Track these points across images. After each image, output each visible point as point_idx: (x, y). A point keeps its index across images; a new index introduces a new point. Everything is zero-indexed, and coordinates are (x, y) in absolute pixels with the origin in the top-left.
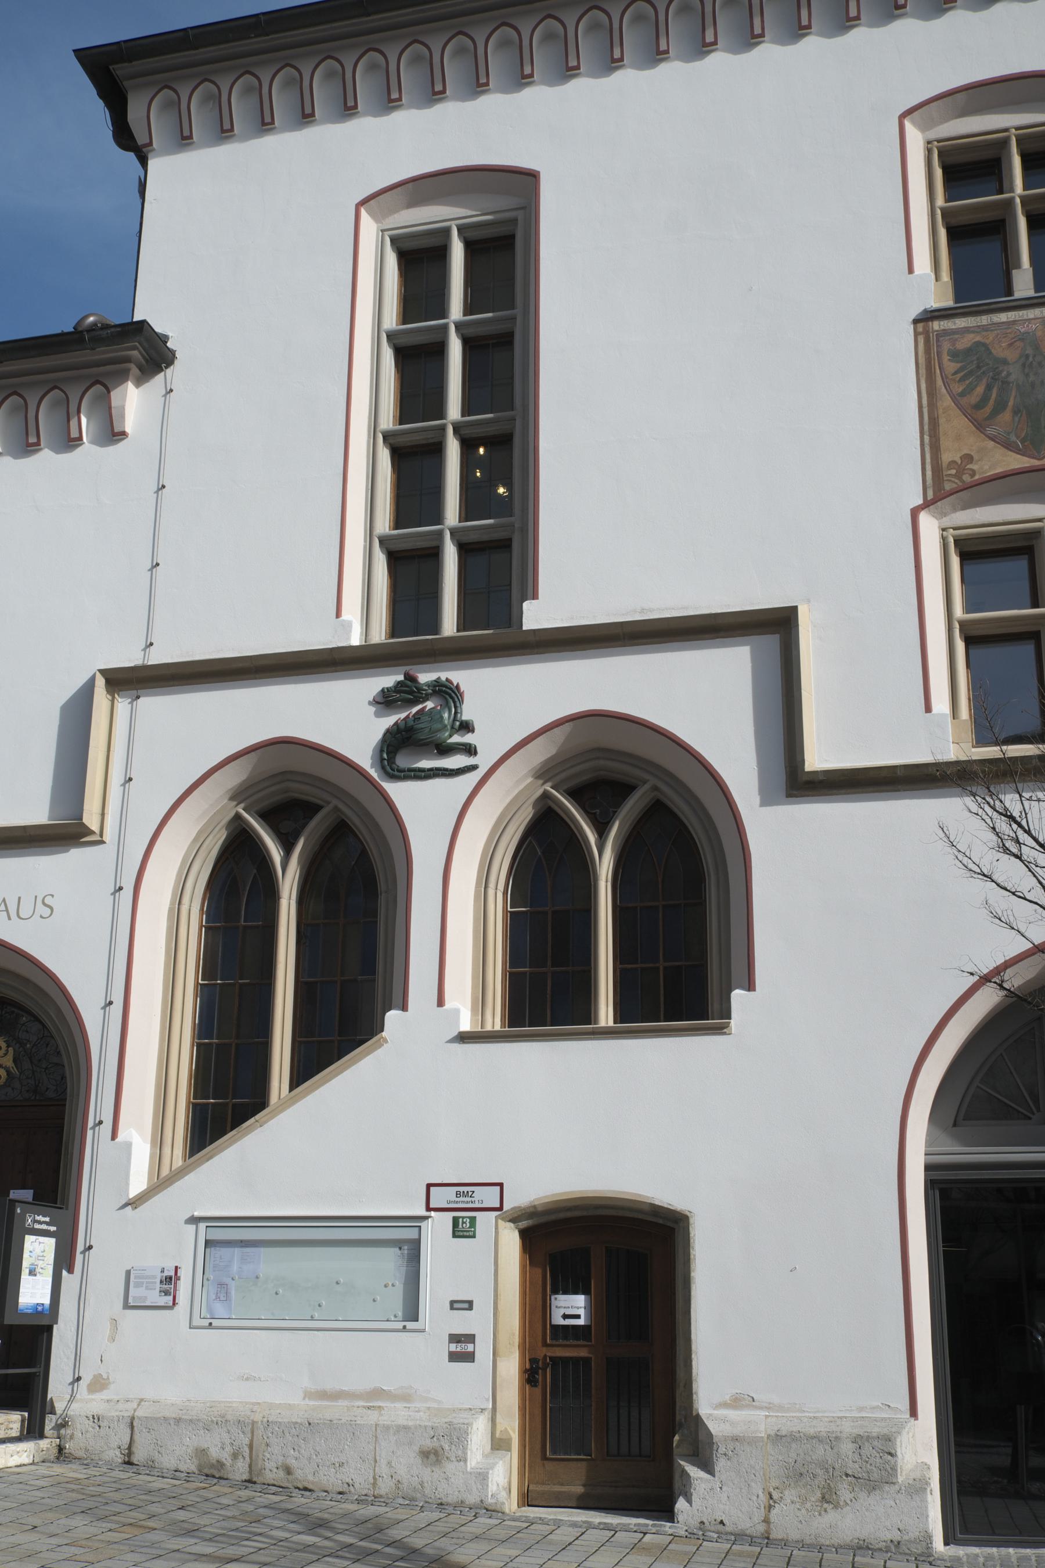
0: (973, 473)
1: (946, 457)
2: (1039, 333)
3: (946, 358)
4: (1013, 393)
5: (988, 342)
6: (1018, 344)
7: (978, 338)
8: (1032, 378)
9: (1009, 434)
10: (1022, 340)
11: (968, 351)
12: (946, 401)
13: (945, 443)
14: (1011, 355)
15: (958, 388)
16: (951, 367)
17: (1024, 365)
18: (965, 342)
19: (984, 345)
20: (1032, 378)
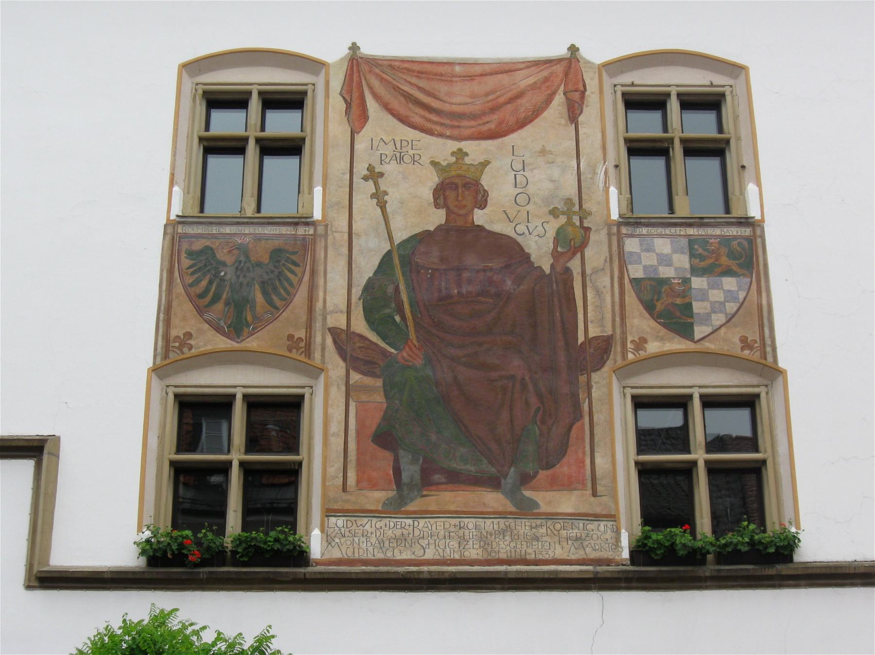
0: (191, 347)
1: (174, 333)
2: (251, 246)
3: (183, 255)
4: (227, 289)
5: (214, 247)
6: (235, 251)
7: (208, 243)
8: (241, 279)
9: (219, 320)
10: (238, 249)
11: (201, 252)
12: (179, 289)
13: (175, 321)
14: (229, 260)
15: (189, 280)
16: (186, 262)
17: (237, 268)
18: (198, 246)
19: (212, 249)
20: (241, 279)
